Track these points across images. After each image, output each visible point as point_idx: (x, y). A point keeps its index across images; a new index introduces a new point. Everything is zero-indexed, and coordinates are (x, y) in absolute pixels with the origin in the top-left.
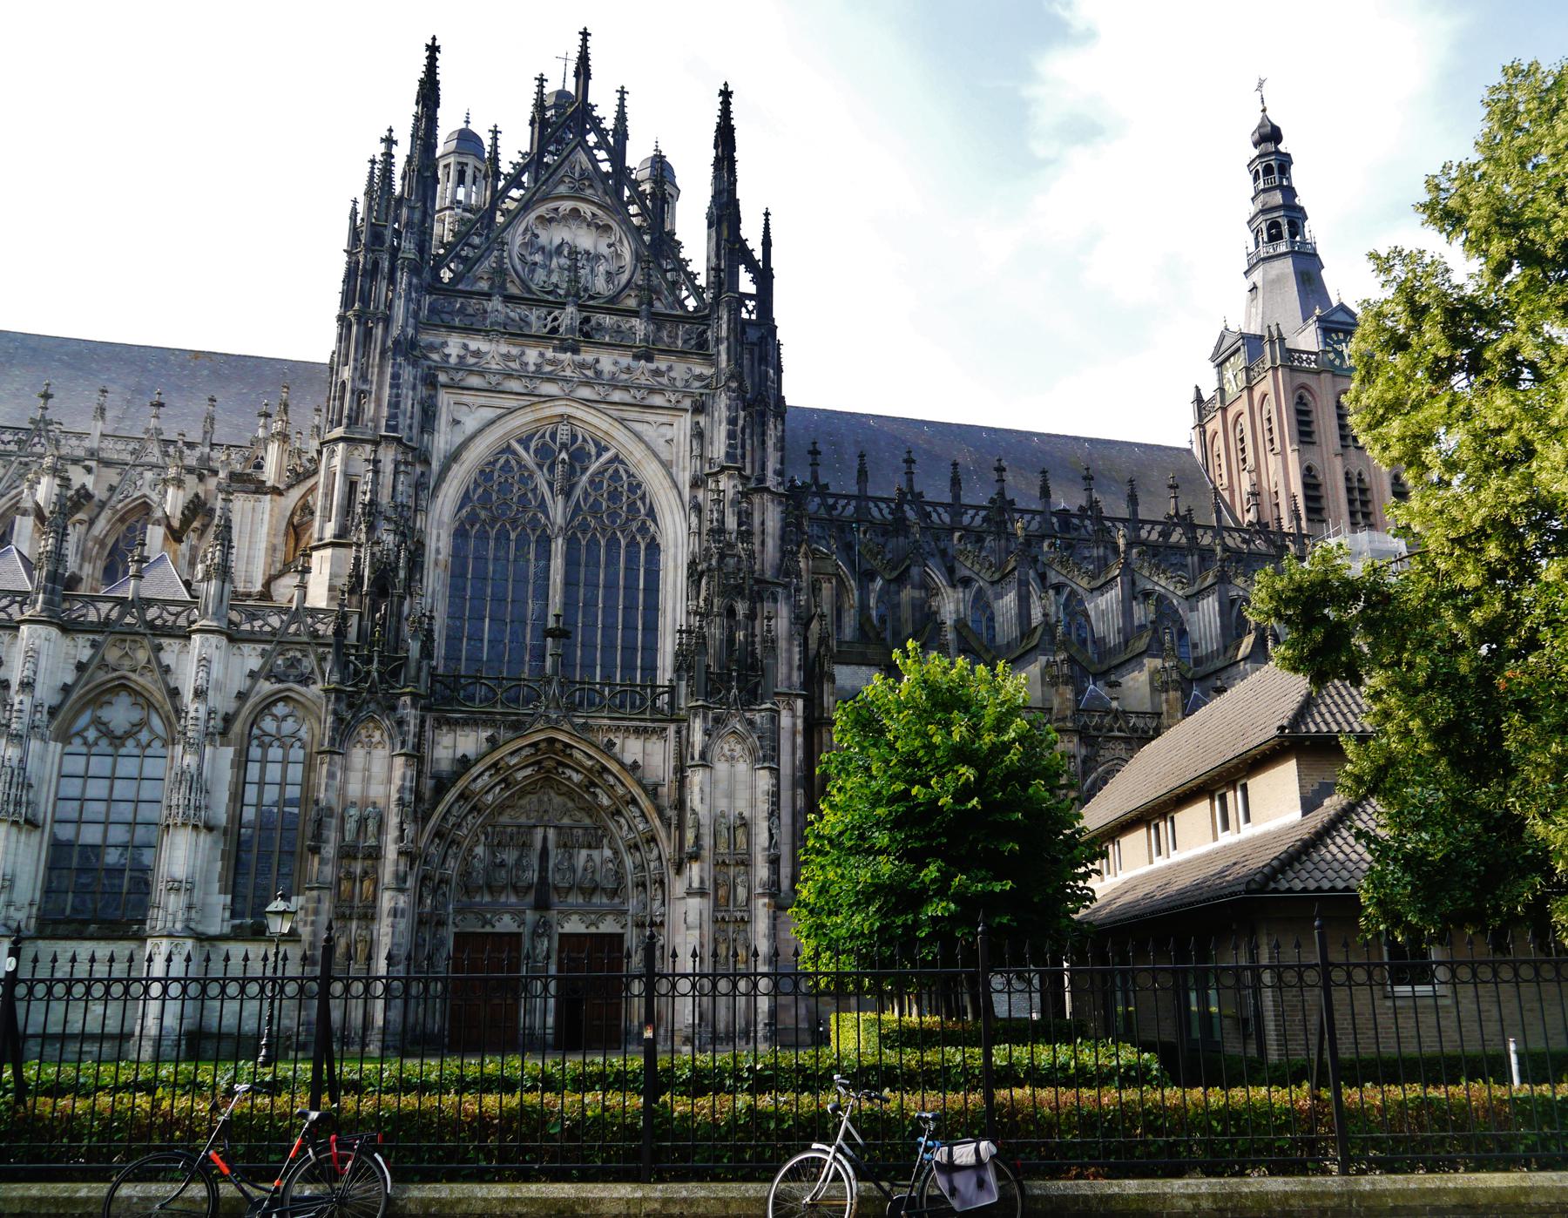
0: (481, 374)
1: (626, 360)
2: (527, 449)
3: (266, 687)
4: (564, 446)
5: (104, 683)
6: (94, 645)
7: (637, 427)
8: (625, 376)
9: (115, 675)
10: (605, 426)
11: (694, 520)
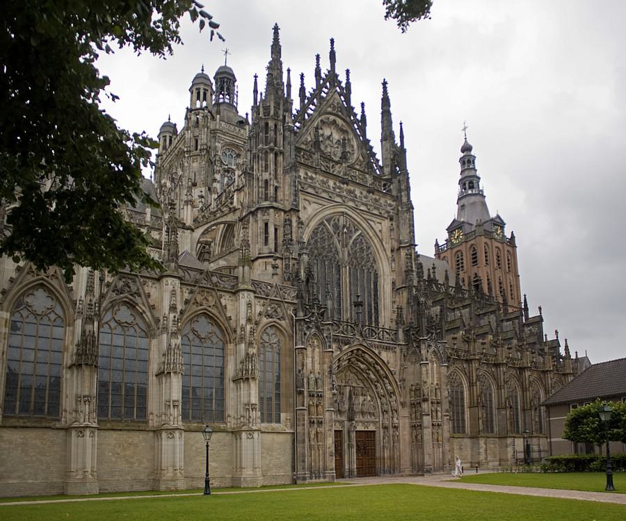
0: (314, 188)
1: (365, 193)
2: (329, 225)
3: (265, 320)
4: (344, 226)
5: (196, 312)
6: (191, 292)
7: (371, 223)
8: (365, 200)
9: (202, 307)
10: (359, 220)
11: (393, 264)
